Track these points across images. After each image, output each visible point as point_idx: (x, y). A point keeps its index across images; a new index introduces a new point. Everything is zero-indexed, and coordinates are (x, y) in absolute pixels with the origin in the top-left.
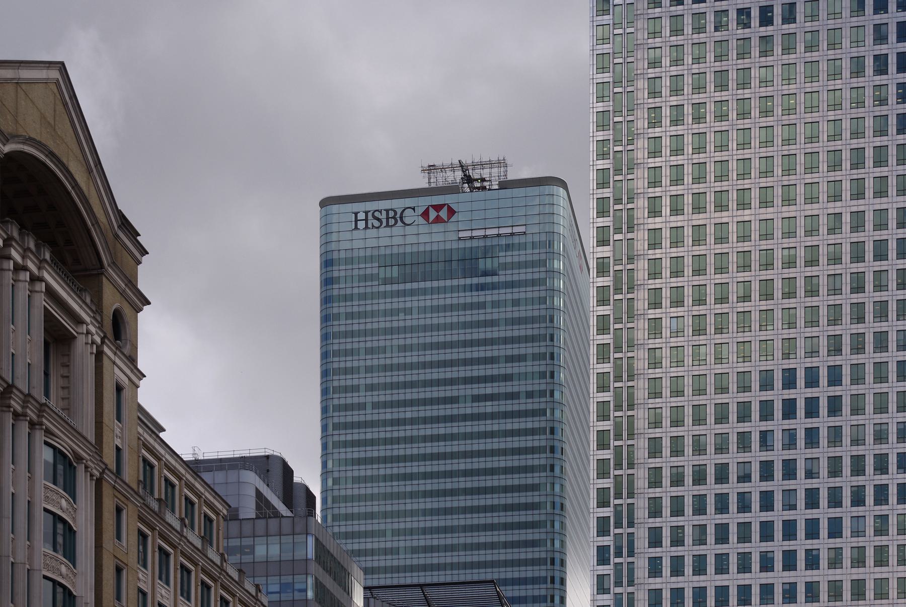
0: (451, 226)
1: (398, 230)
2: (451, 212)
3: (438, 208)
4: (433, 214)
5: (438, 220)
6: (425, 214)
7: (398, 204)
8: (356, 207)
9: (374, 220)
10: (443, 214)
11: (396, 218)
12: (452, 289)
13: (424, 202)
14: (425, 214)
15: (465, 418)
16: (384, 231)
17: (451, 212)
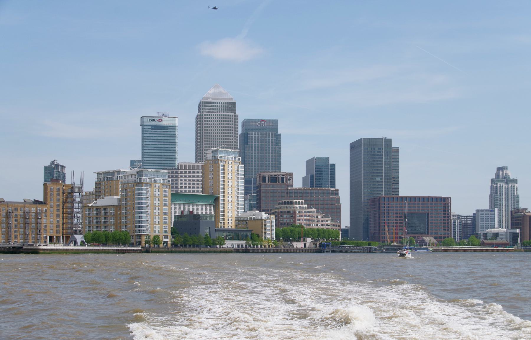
0: (161, 122)
1: (154, 122)
2: (162, 120)
3: (160, 119)
4: (159, 120)
5: (160, 121)
6: (158, 120)
7: (154, 118)
8: (148, 118)
9: (150, 120)
10: (161, 120)
11: (153, 120)
12: (162, 131)
13: (158, 118)
14: (158, 120)
15: (163, 150)
16: (152, 122)
17: (162, 120)
